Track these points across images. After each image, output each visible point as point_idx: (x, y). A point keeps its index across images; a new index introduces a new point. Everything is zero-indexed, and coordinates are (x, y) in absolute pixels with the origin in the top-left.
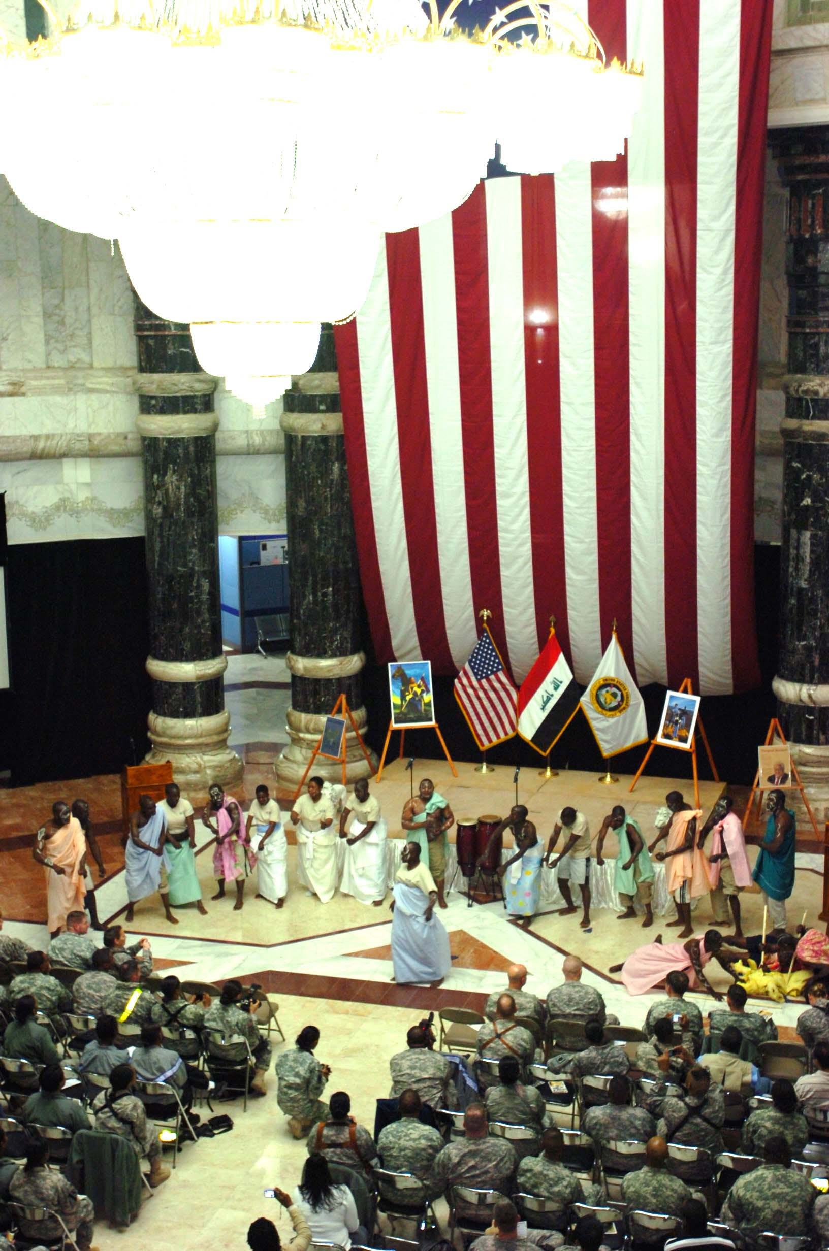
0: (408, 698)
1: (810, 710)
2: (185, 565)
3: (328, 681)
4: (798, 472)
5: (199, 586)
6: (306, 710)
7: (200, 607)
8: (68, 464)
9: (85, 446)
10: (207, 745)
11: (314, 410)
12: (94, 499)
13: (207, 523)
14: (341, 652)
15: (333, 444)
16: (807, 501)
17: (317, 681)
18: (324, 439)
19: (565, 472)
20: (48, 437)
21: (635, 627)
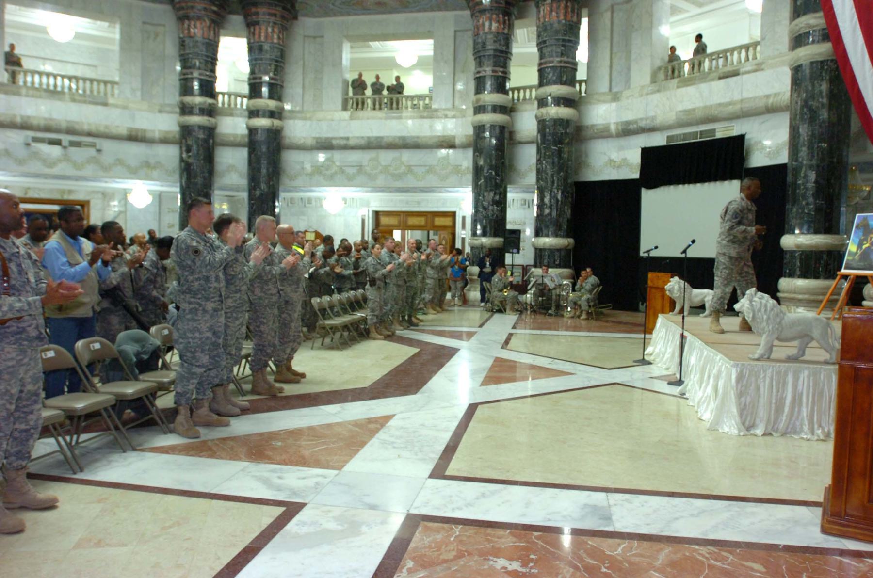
0: (864, 247)
2: (796, 161)
5: (806, 176)
7: (805, 193)
10: (800, 300)
13: (817, 127)
20: (776, 95)
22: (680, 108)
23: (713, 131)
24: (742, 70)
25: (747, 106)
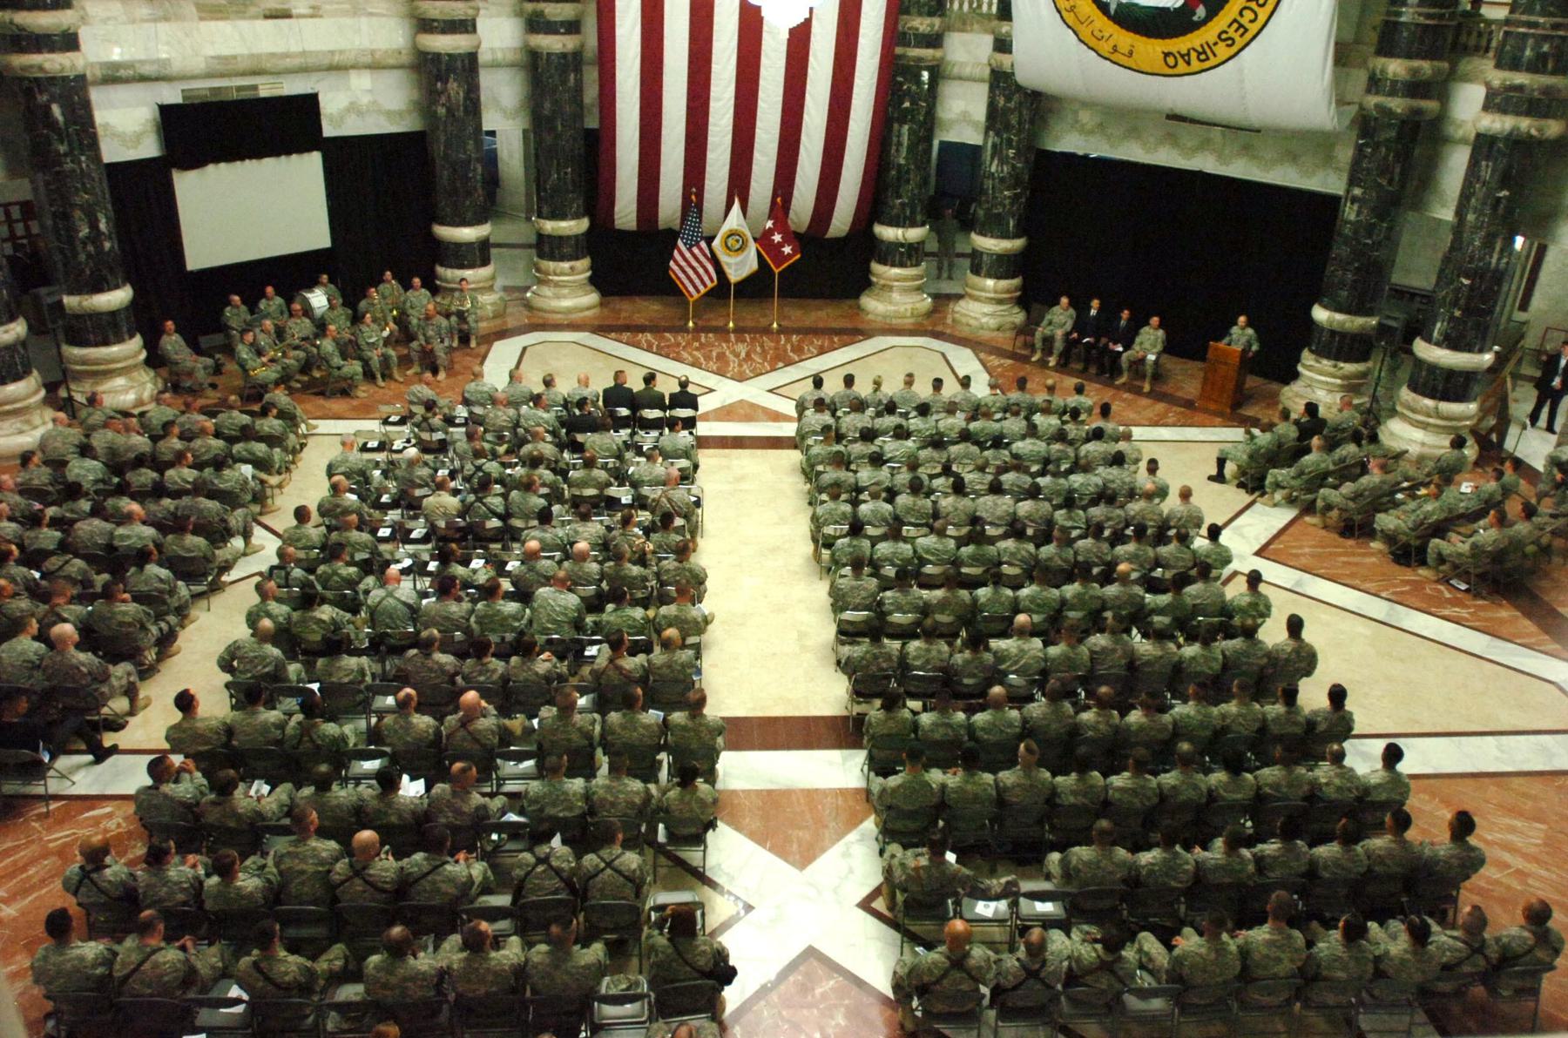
1: (902, 245)
3: (569, 237)
4: (901, 84)
6: (552, 258)
8: (353, 73)
9: (368, 59)
11: (556, 32)
12: (375, 102)
14: (576, 216)
15: (570, 58)
16: (907, 104)
17: (561, 238)
18: (564, 56)
19: (762, 82)
20: (341, 52)
21: (796, 192)
22: (210, 51)
23: (255, 88)
24: (294, 12)
25: (311, 61)
